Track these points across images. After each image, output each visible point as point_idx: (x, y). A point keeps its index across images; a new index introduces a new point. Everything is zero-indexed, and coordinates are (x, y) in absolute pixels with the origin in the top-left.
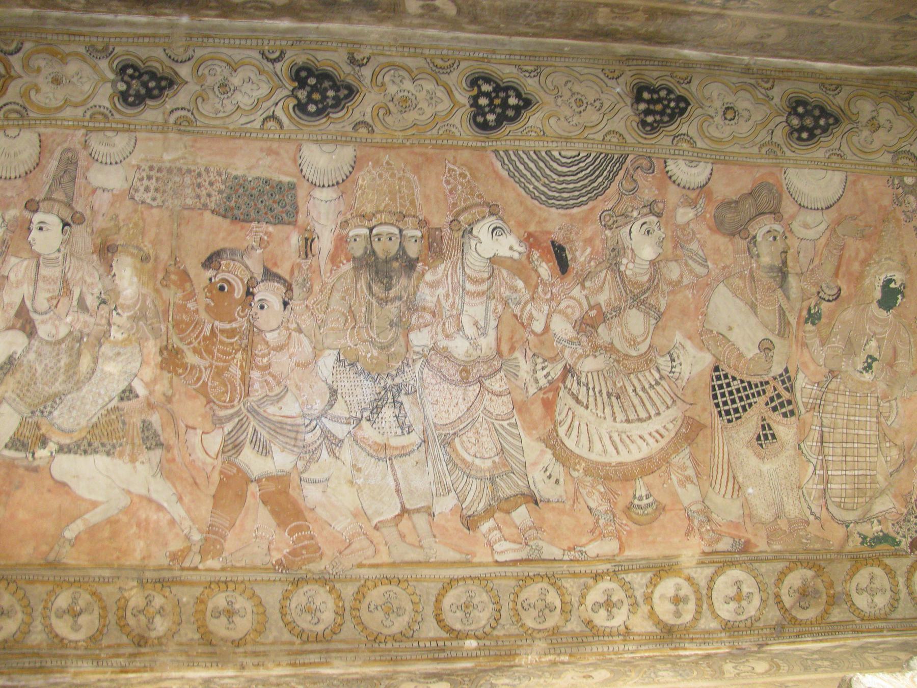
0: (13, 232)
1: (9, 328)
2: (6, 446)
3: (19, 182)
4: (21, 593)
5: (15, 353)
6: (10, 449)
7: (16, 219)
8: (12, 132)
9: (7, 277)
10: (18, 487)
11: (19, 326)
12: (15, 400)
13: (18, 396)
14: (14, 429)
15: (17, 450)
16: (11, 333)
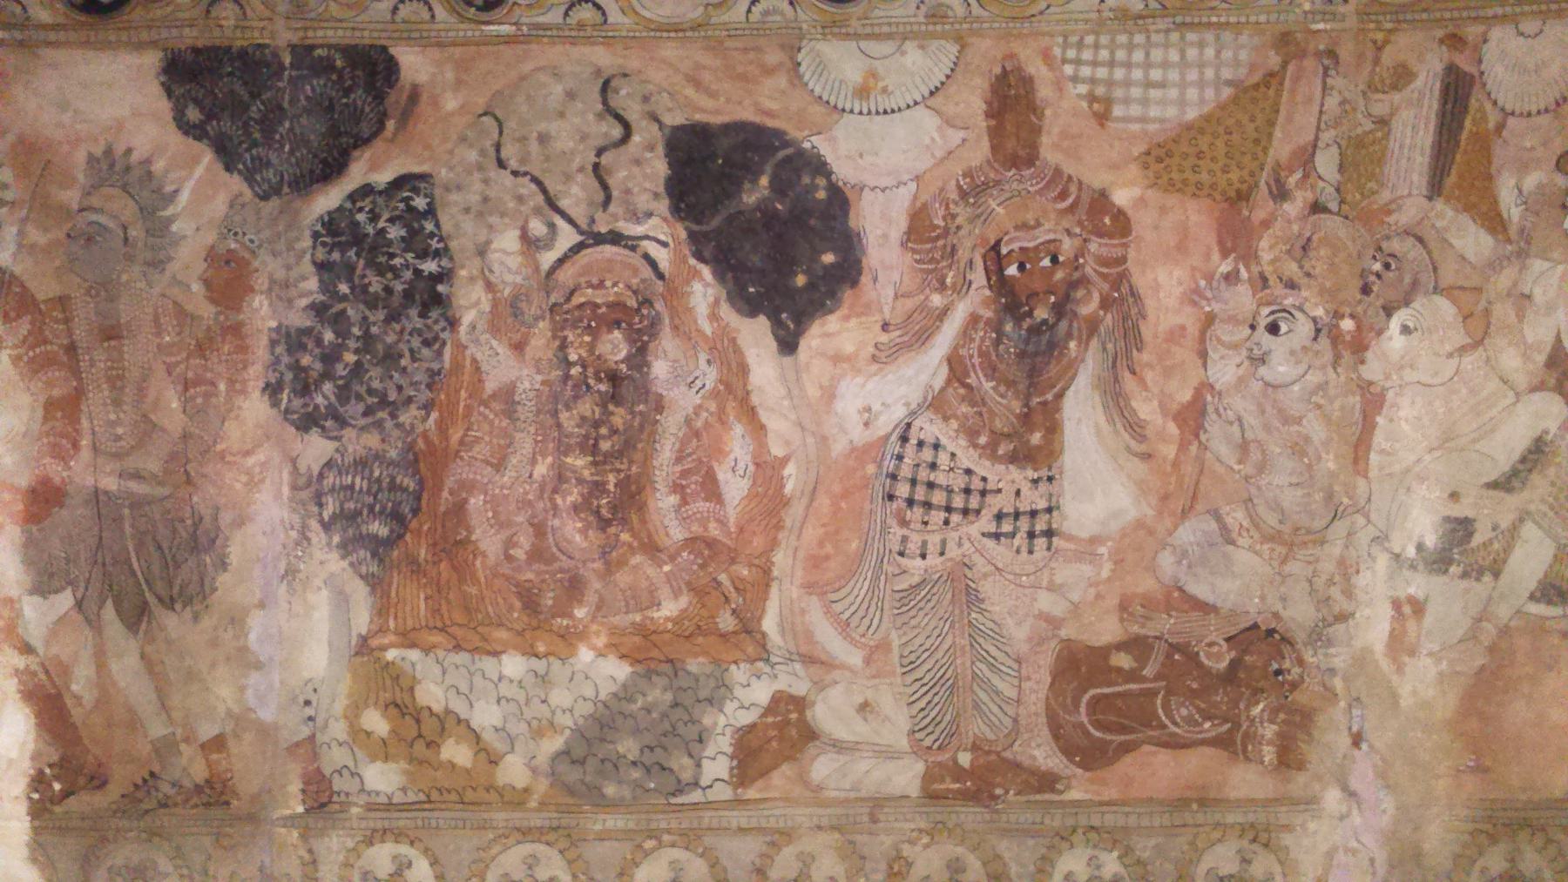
0: (1537, 214)
1: (1534, 389)
2: (1532, 597)
3: (1544, 120)
4: (1552, 850)
5: (1547, 433)
6: (1538, 601)
7: (1540, 186)
8: (1529, 26)
9: (1529, 297)
10: (1550, 668)
11: (1552, 382)
12: (1545, 515)
13: (1552, 508)
14: (1544, 567)
15: (1550, 602)
16: (1537, 396)
